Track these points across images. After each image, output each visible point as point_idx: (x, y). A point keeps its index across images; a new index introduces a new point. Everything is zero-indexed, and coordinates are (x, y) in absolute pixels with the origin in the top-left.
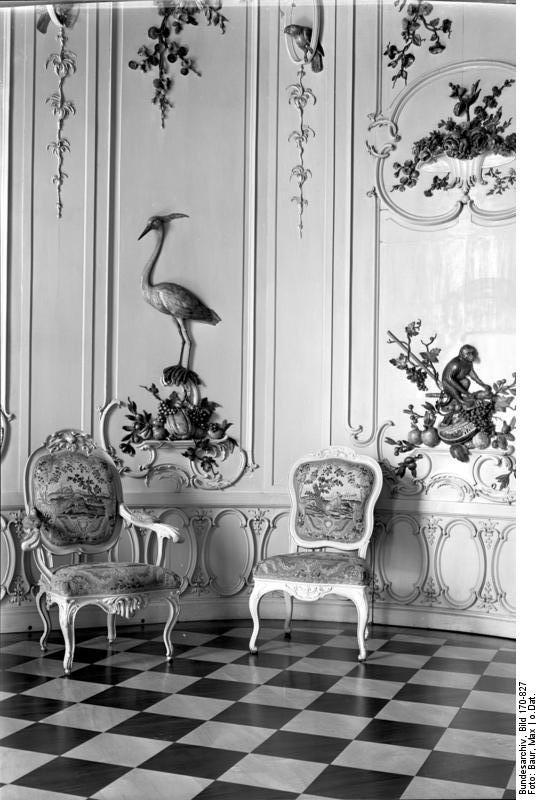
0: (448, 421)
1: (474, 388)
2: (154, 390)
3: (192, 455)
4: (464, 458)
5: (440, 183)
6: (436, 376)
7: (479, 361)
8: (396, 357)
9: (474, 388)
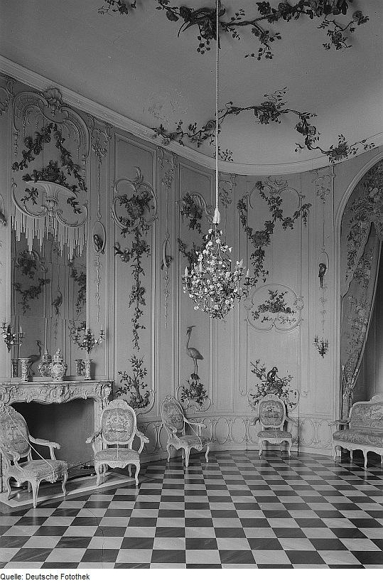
3: (198, 401)
5: (265, 319)
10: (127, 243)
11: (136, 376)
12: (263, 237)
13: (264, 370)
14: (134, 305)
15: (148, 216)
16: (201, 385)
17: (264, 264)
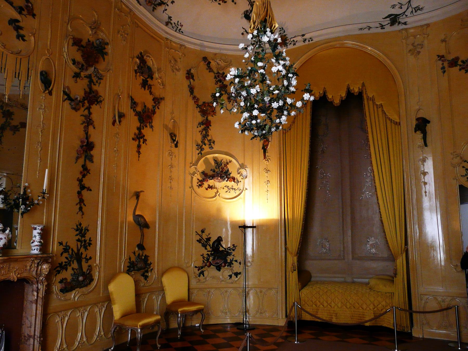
0: (214, 259)
1: (221, 249)
2: (134, 253)
3: (143, 275)
4: (219, 271)
5: (210, 187)
6: (210, 246)
7: (222, 241)
8: (198, 239)
9: (221, 249)
10: (78, 90)
11: (79, 247)
12: (206, 110)
13: (209, 239)
14: (81, 161)
15: (101, 66)
16: (146, 257)
17: (210, 133)
